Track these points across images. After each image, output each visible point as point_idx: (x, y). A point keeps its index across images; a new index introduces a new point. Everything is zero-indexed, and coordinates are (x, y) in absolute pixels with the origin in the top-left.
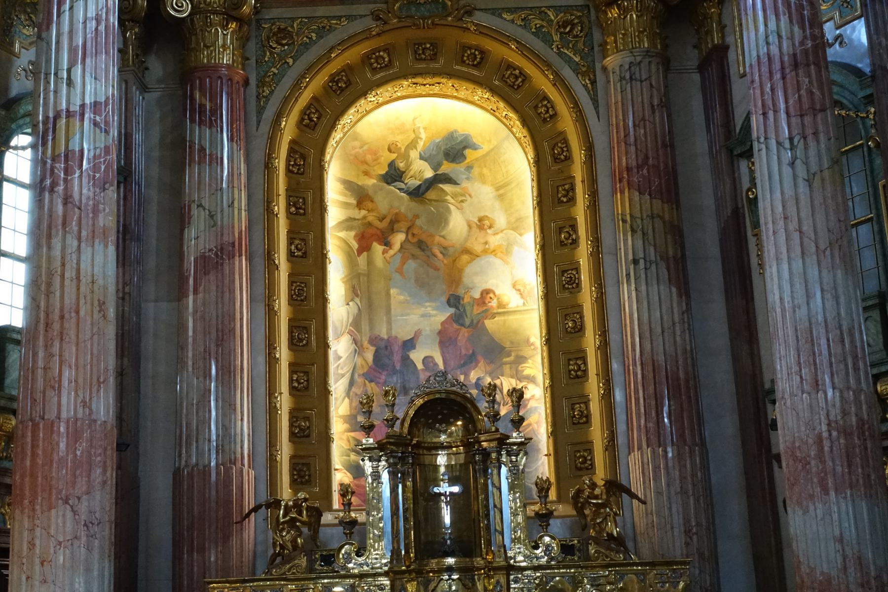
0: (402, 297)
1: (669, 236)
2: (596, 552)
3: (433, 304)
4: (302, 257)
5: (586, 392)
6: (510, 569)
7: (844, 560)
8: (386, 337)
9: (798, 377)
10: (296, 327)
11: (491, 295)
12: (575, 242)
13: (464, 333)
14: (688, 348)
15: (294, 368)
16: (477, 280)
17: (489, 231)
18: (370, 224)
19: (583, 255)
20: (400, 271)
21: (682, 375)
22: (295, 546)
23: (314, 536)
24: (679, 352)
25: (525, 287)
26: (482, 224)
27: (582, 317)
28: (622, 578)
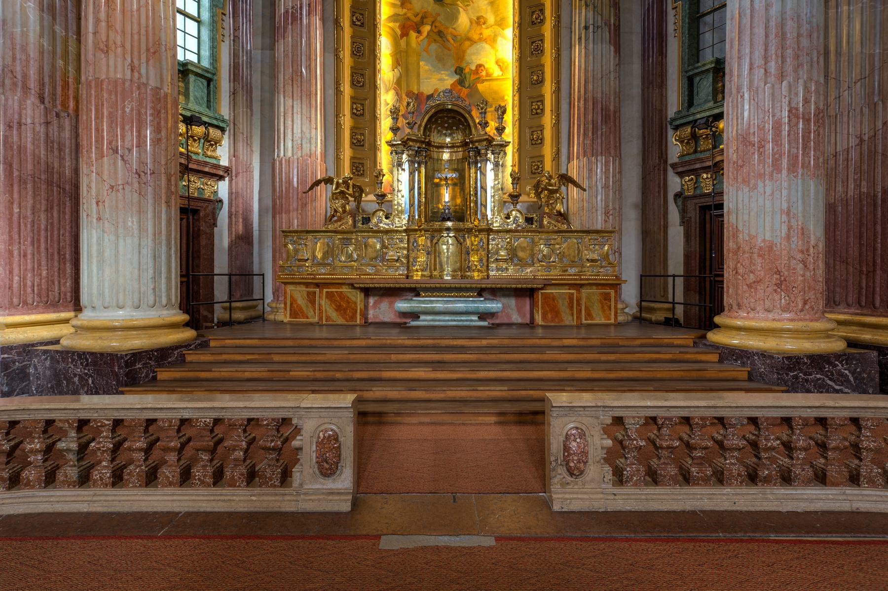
0: (427, 67)
1: (612, 9)
2: (548, 223)
3: (446, 72)
4: (360, 26)
5: (542, 123)
6: (489, 231)
7: (789, 229)
8: (416, 92)
9: (762, 71)
10: (355, 73)
11: (482, 68)
12: (542, 21)
13: (465, 91)
14: (617, 90)
15: (354, 100)
16: (474, 58)
17: (483, 26)
18: (408, 18)
19: (547, 30)
20: (426, 50)
21: (612, 108)
22: (344, 211)
23: (358, 207)
24: (612, 92)
25: (503, 64)
26: (479, 21)
27: (543, 73)
28: (566, 241)
